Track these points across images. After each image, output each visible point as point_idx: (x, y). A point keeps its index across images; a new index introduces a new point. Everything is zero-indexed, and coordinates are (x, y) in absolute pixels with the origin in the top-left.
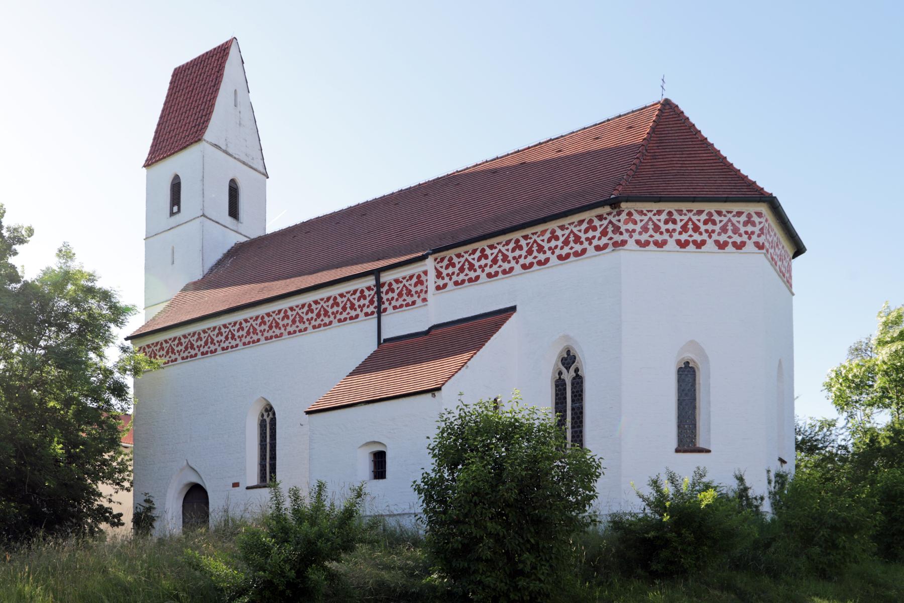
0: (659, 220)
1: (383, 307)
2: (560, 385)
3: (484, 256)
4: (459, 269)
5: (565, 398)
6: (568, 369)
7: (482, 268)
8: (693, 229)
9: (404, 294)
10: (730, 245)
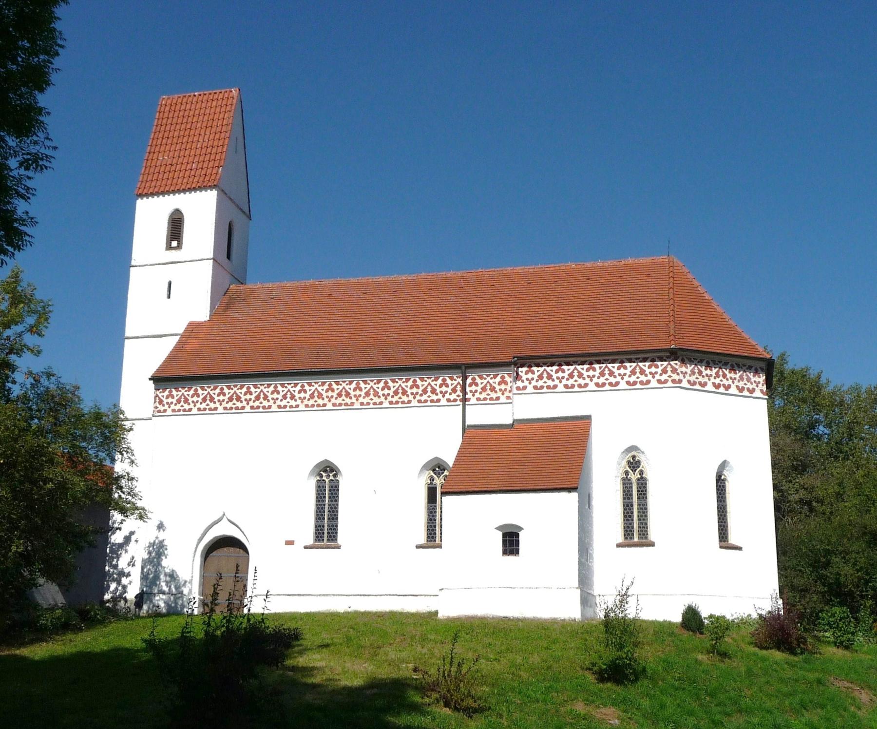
0: (378, 388)
1: (467, 396)
2: (626, 484)
3: (330, 389)
4: (310, 395)
5: (631, 495)
6: (634, 471)
7: (195, 403)
8: (402, 393)
9: (488, 390)
10: (746, 390)
